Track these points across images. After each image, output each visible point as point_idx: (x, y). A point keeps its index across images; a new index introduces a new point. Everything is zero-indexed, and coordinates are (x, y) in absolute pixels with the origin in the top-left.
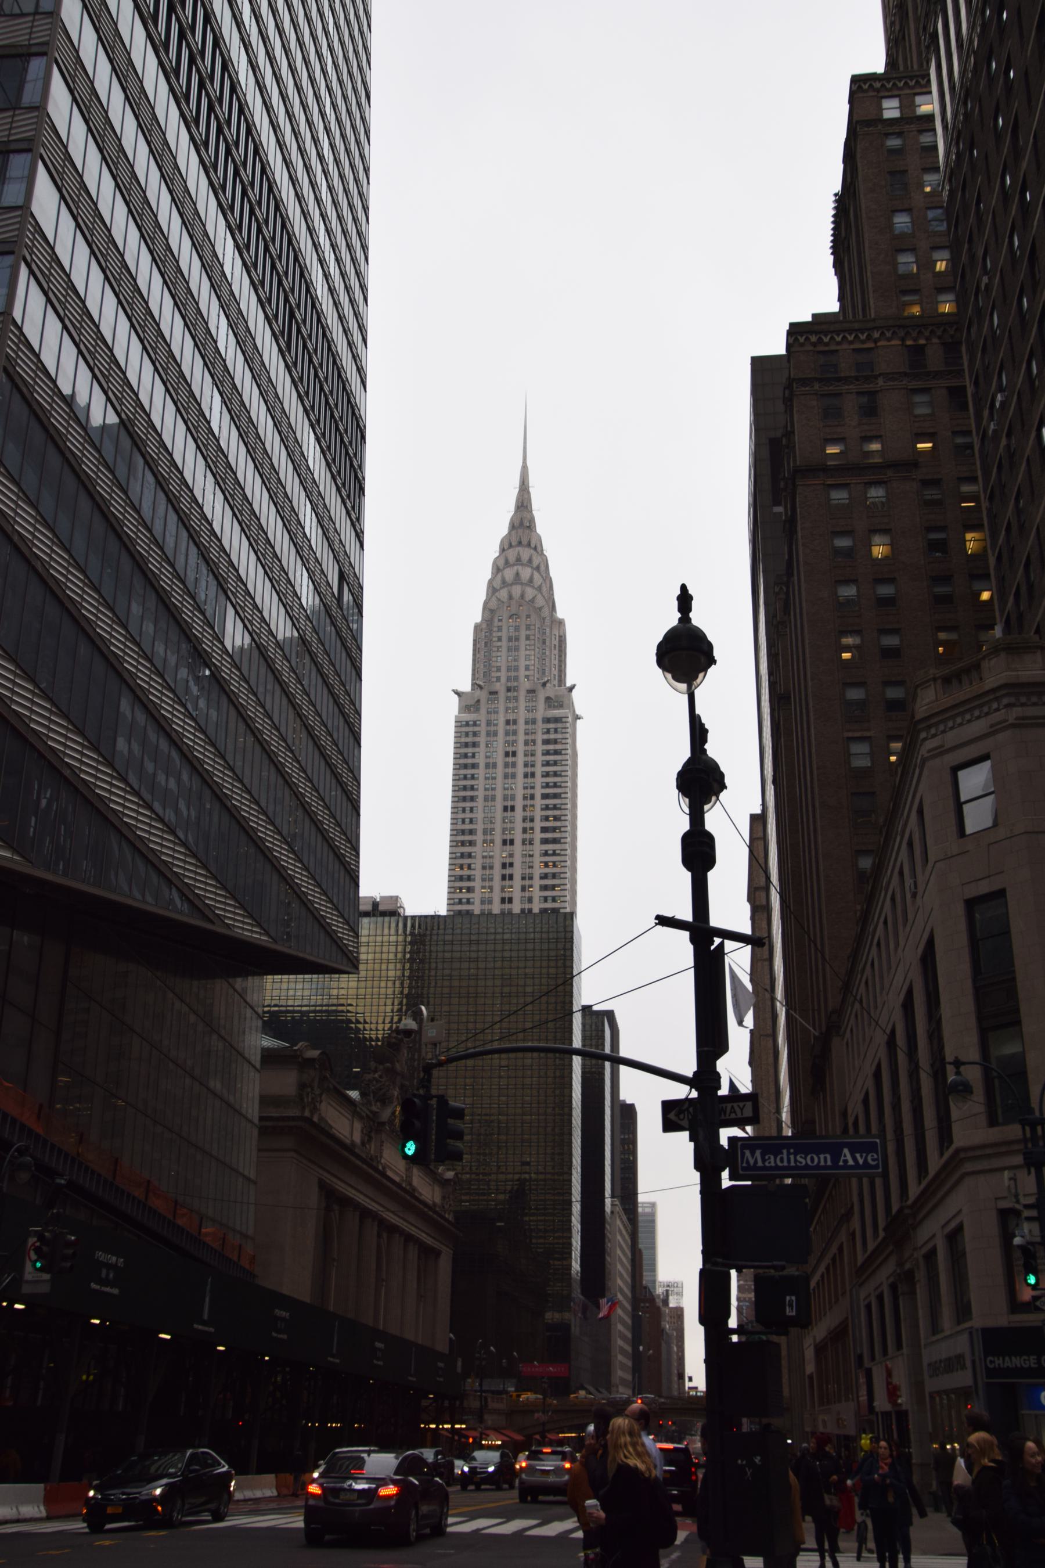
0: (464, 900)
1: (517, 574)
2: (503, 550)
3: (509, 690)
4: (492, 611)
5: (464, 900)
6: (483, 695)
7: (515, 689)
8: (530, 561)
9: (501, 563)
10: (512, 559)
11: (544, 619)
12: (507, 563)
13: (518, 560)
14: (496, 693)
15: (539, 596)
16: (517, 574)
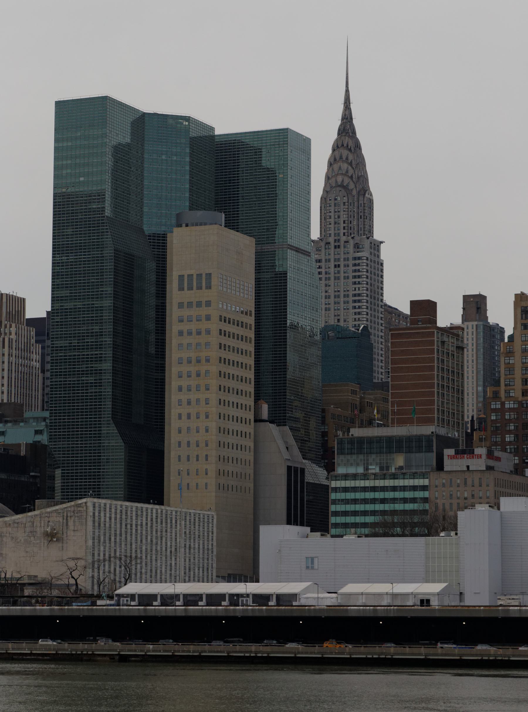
0: (357, 319)
1: (340, 168)
2: (334, 150)
3: (335, 241)
4: (327, 192)
5: (357, 319)
6: (323, 244)
7: (339, 241)
8: (347, 159)
9: (332, 161)
10: (338, 158)
11: (354, 196)
12: (335, 160)
13: (341, 158)
14: (329, 243)
15: (351, 182)
16: (340, 168)
